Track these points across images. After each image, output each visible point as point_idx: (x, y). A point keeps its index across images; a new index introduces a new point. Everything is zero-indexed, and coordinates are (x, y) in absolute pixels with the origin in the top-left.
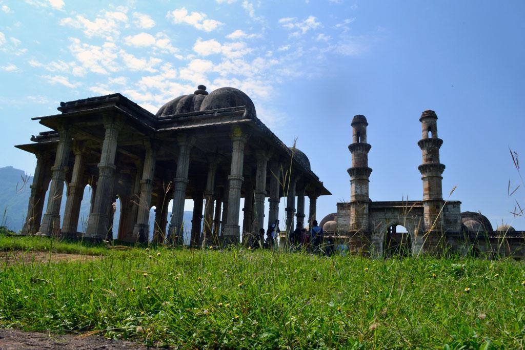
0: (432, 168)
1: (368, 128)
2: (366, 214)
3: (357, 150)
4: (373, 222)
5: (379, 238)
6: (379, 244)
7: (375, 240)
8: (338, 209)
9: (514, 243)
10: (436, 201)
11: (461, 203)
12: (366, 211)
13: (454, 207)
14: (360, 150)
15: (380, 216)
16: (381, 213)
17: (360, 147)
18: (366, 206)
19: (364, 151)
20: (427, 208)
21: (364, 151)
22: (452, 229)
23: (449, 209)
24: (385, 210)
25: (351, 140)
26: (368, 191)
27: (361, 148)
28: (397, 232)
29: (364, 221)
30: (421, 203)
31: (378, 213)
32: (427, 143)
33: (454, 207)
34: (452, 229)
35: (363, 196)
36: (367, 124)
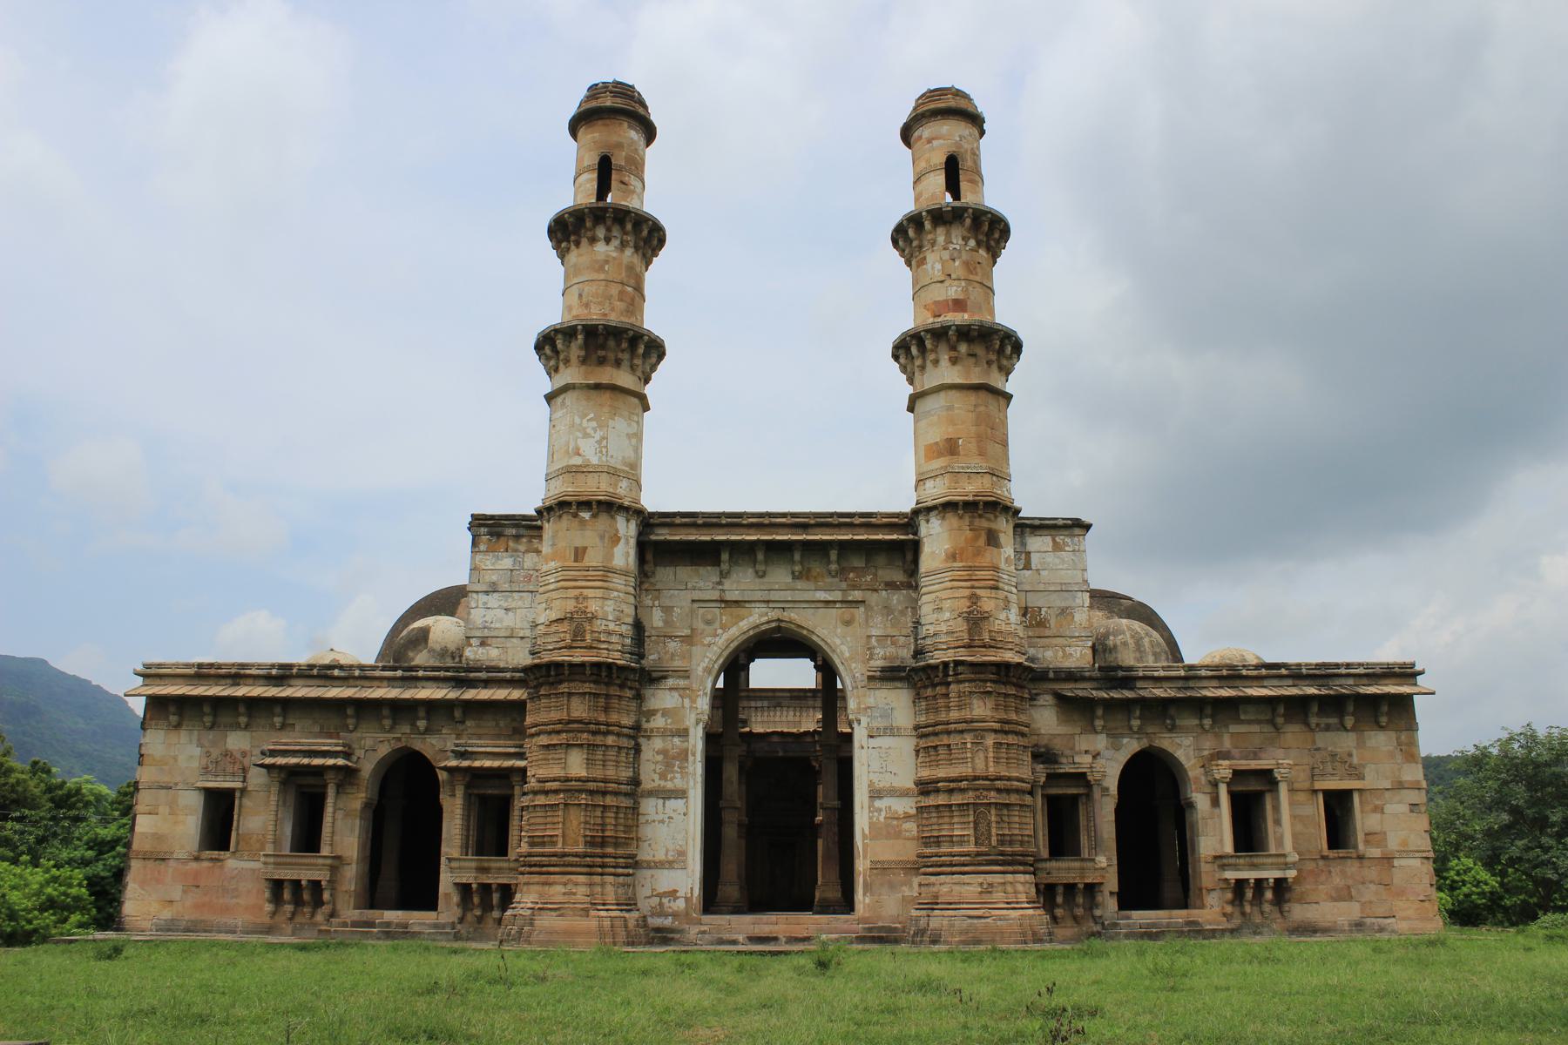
0: (963, 348)
1: (652, 155)
2: (625, 573)
3: (593, 240)
4: (656, 620)
5: (687, 702)
6: (684, 733)
7: (665, 713)
8: (474, 544)
9: (1324, 721)
10: (987, 504)
11: (1088, 527)
12: (624, 555)
13: (1057, 547)
14: (608, 240)
15: (686, 589)
16: (702, 570)
17: (609, 230)
18: (627, 529)
19: (629, 252)
20: (936, 539)
21: (629, 252)
22: (1049, 654)
23: (1035, 559)
24: (725, 556)
25: (566, 190)
26: (637, 450)
27: (616, 232)
28: (752, 686)
29: (610, 607)
30: (909, 522)
31: (684, 572)
32: (941, 231)
33: (1057, 547)
34: (1049, 654)
35: (613, 473)
36: (650, 133)
